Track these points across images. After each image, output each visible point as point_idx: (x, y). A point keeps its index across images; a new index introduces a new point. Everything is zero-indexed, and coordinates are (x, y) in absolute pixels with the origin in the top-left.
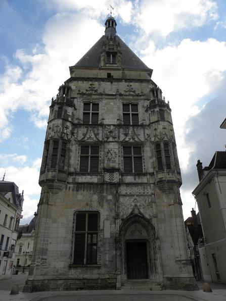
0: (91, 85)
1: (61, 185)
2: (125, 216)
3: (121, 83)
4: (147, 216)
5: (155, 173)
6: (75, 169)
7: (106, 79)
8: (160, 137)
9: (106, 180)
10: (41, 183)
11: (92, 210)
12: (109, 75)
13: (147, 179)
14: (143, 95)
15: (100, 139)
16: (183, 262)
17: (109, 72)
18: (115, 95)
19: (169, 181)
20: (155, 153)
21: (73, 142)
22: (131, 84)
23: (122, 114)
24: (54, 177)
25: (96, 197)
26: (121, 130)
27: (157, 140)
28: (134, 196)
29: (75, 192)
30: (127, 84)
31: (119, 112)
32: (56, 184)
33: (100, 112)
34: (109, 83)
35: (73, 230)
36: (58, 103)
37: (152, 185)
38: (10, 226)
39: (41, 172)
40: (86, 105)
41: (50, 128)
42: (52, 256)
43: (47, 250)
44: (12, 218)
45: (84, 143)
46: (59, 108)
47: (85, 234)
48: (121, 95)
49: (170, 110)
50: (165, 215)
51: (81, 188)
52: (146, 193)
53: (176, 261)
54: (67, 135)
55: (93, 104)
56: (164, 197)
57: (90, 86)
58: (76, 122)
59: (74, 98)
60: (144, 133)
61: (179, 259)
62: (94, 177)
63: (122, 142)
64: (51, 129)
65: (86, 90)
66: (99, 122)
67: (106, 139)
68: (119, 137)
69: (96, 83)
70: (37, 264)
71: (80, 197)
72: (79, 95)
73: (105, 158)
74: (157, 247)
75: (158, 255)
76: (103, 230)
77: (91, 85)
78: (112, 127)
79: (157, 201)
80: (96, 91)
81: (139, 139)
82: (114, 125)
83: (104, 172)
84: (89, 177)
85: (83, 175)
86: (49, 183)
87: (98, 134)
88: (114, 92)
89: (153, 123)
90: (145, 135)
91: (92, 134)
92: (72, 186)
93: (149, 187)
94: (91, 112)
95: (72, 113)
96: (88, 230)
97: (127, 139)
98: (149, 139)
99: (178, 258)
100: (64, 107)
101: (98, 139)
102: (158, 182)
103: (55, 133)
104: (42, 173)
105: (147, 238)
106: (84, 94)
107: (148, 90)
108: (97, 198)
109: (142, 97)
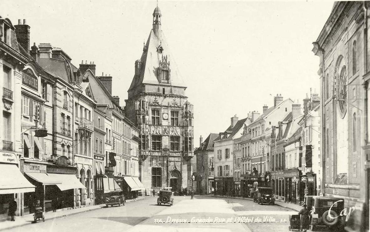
12: (164, 89)
17: (164, 88)
40: (153, 111)
46: (143, 116)
48: (171, 107)
77: (155, 99)
78: (166, 127)
81: (177, 134)
92: (150, 157)
101: (160, 134)
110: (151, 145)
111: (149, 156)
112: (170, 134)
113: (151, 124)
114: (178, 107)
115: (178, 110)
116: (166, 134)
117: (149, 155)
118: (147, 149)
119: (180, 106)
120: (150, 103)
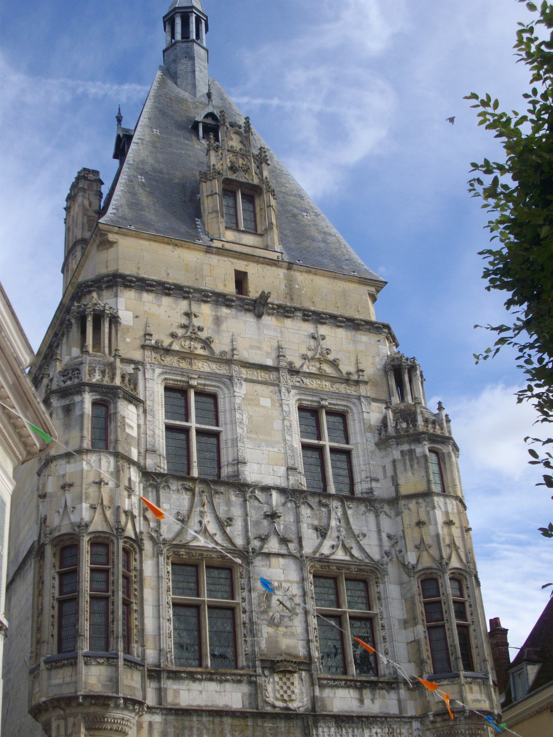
0: (188, 315)
1: (127, 715)
3: (288, 322)
8: (437, 557)
9: (271, 700)
13: (399, 701)
14: (366, 383)
15: (239, 542)
17: (241, 266)
18: (276, 369)
20: (420, 608)
21: (148, 546)
26: (305, 511)
27: (426, 562)
34: (250, 318)
36: (94, 388)
37: (416, 725)
45: (182, 551)
46: (95, 404)
48: (293, 372)
49: (456, 448)
51: (191, 728)
55: (197, 394)
57: (184, 320)
58: (150, 463)
60: (379, 531)
62: (228, 686)
65: (173, 336)
66: (226, 471)
67: (256, 543)
68: (300, 540)
72: (148, 353)
77: (188, 315)
78: (274, 494)
81: (362, 549)
82: (282, 491)
83: (263, 668)
84: (212, 686)
85: (192, 676)
86: (92, 710)
89: (409, 497)
92: (157, 718)
95: (139, 426)
97: (326, 550)
102: (436, 715)
110: (168, 627)
111: (150, 709)
112: (308, 549)
113: (164, 467)
114: (347, 381)
115: (347, 397)
116: (273, 545)
117: (151, 700)
118: (128, 650)
119: (355, 377)
120: (148, 335)
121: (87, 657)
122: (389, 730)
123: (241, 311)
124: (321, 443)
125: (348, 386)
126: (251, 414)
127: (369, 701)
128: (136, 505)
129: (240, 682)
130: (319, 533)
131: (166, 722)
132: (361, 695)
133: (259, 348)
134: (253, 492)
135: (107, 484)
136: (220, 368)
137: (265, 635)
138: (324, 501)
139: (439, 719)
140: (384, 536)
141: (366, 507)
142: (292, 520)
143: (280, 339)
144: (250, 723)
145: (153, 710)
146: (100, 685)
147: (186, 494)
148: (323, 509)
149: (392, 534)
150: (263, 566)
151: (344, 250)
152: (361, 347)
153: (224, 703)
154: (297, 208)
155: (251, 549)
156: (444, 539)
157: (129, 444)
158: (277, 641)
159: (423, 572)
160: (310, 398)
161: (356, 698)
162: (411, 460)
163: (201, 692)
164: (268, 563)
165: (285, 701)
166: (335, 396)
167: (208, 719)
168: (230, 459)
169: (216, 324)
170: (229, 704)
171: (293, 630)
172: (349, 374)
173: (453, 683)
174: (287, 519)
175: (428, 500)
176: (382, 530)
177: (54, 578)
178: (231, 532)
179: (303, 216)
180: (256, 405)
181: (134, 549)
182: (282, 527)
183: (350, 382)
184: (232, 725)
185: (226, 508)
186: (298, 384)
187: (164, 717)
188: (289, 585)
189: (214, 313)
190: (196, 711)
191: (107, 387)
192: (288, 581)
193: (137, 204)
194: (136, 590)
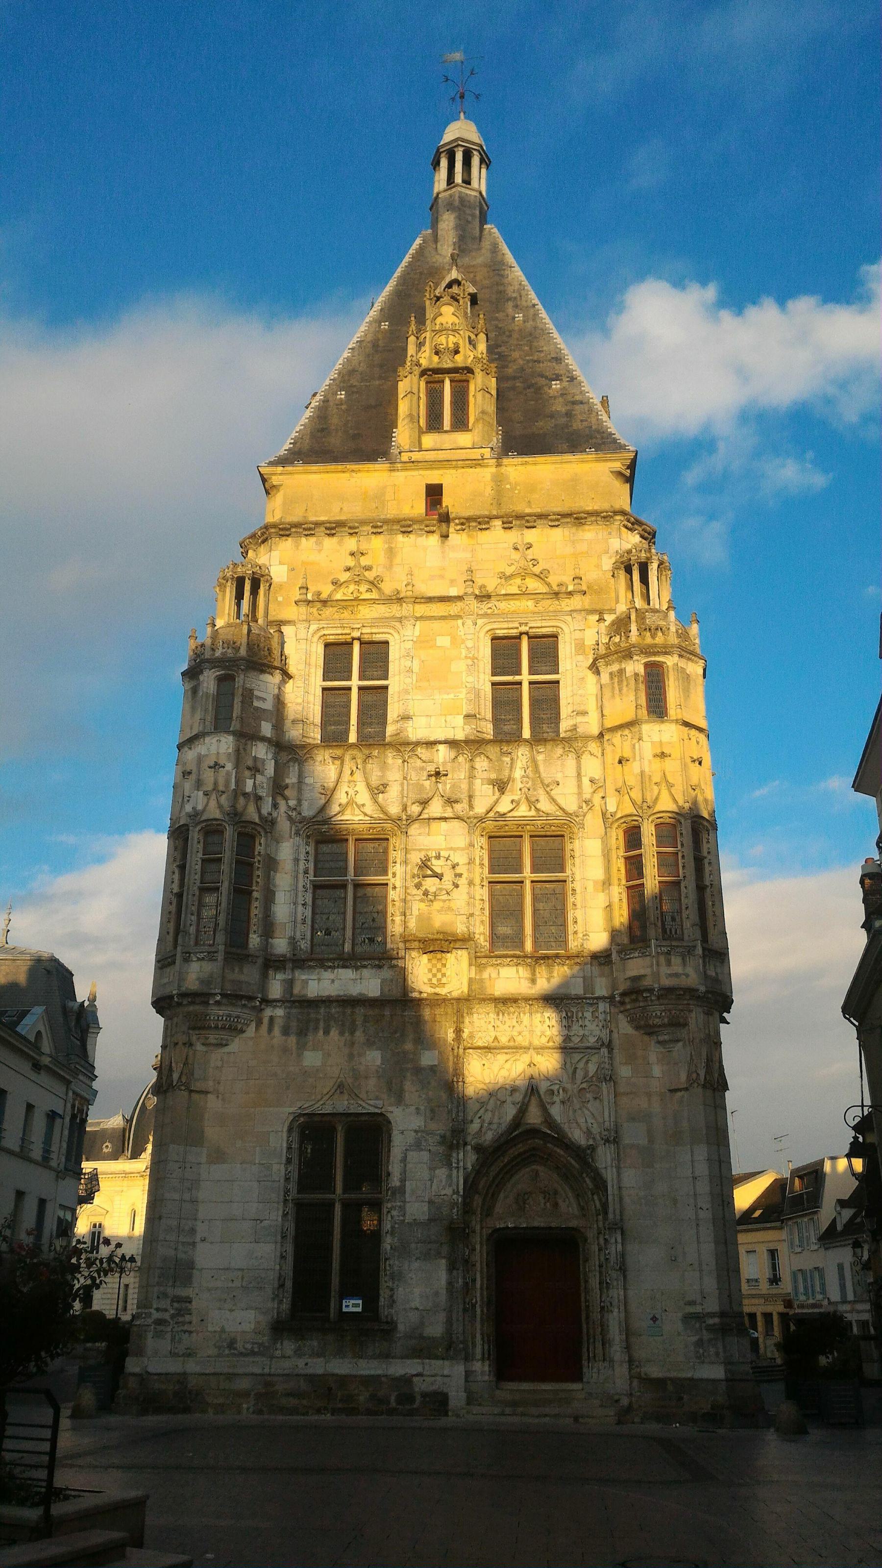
1: (236, 1011)
2: (489, 1136)
3: (484, 536)
4: (577, 1136)
5: (614, 956)
6: (293, 941)
7: (415, 521)
8: (639, 801)
10: (161, 1004)
11: (360, 1110)
12: (434, 493)
15: (394, 810)
16: (711, 1321)
17: (434, 477)
18: (460, 598)
19: (667, 992)
20: (619, 865)
22: (530, 536)
23: (488, 688)
24: (206, 982)
25: (374, 1058)
26: (481, 763)
27: (629, 809)
28: (526, 1049)
29: (292, 1040)
30: (513, 536)
31: (470, 679)
32: (218, 1012)
33: (395, 683)
34: (434, 540)
35: (287, 1192)
36: (215, 663)
37: (602, 1006)
38: (46, 1158)
39: (158, 961)
41: (186, 774)
42: (209, 1290)
43: (190, 1265)
44: (52, 1116)
46: (220, 680)
47: (332, 1205)
48: (484, 597)
50: (649, 1131)
51: (318, 1020)
52: (576, 1040)
53: (688, 1318)
54: (259, 798)
56: (653, 1058)
57: (351, 562)
59: (280, 623)
60: (579, 775)
61: (698, 1309)
62: (366, 972)
63: (481, 819)
64: (193, 777)
66: (390, 730)
67: (415, 809)
68: (470, 797)
69: (377, 544)
70: (156, 1315)
71: (312, 1059)
72: (303, 609)
73: (414, 891)
74: (613, 1258)
75: (617, 1293)
76: (402, 1190)
78: (441, 747)
79: (624, 1071)
80: (374, 584)
81: (553, 800)
82: (452, 743)
84: (347, 974)
87: (383, 788)
88: (452, 582)
90: (580, 786)
91: (361, 787)
92: (280, 1012)
93: (588, 1015)
94: (355, 682)
96: (345, 1190)
97: (504, 806)
98: (597, 800)
99: (692, 1303)
100: (240, 680)
102: (624, 994)
103: (206, 794)
104: (164, 962)
105: (573, 1223)
106: (324, 602)
107: (607, 563)
108: (378, 1062)
109: (576, 602)
121: (186, 953)
122: (567, 1015)
123: (422, 535)
124: (517, 678)
125: (558, 599)
126: (423, 659)
127: (544, 980)
128: (265, 785)
129: (380, 967)
130: (496, 788)
131: (288, 1017)
132: (533, 973)
133: (442, 577)
134: (412, 750)
135: (224, 767)
136: (390, 611)
137: (415, 912)
138: (505, 749)
139: (627, 1000)
140: (586, 781)
141: (564, 748)
142: (462, 777)
143: (471, 560)
144: (387, 1013)
145: (275, 1004)
146: (197, 982)
147: (333, 763)
148: (507, 759)
149: (597, 778)
150: (420, 834)
151: (594, 420)
152: (583, 547)
153: (358, 991)
154: (546, 378)
155: (404, 817)
156: (650, 776)
157: (258, 719)
158: (429, 919)
159: (622, 821)
160: (505, 625)
161: (526, 978)
162: (620, 682)
163: (333, 981)
164: (427, 830)
165: (433, 986)
166: (538, 617)
167: (338, 1010)
168: (395, 716)
169: (388, 558)
170: (365, 992)
171: (453, 905)
172: (560, 585)
173: (644, 955)
174: (455, 776)
175: (635, 729)
176: (583, 773)
177: (174, 873)
178: (384, 799)
179: (550, 387)
180: (431, 647)
181: (259, 832)
182: (448, 786)
183: (561, 595)
184: (365, 1016)
185: (379, 774)
186: (489, 611)
187: (288, 1010)
188: (452, 853)
189: (386, 546)
190: (323, 1001)
191: (230, 660)
192: (451, 849)
193: (323, 430)
194: (258, 876)
